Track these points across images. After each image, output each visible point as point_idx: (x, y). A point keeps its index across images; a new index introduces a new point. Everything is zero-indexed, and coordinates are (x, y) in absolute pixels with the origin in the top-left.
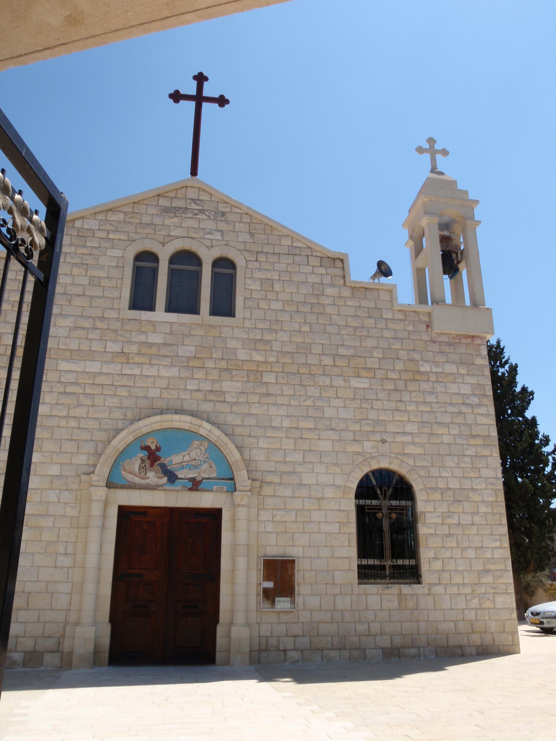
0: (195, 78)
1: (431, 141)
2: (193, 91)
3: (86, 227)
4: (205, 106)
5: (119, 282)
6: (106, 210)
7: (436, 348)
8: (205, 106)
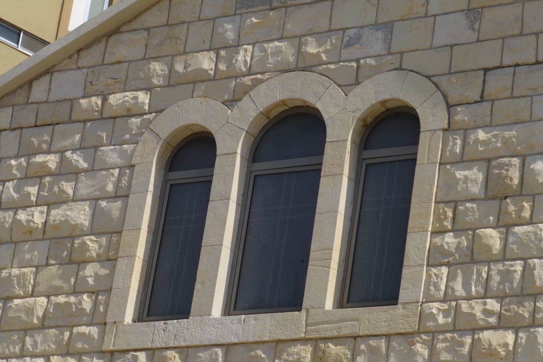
3: (57, 94)
6: (103, 36)
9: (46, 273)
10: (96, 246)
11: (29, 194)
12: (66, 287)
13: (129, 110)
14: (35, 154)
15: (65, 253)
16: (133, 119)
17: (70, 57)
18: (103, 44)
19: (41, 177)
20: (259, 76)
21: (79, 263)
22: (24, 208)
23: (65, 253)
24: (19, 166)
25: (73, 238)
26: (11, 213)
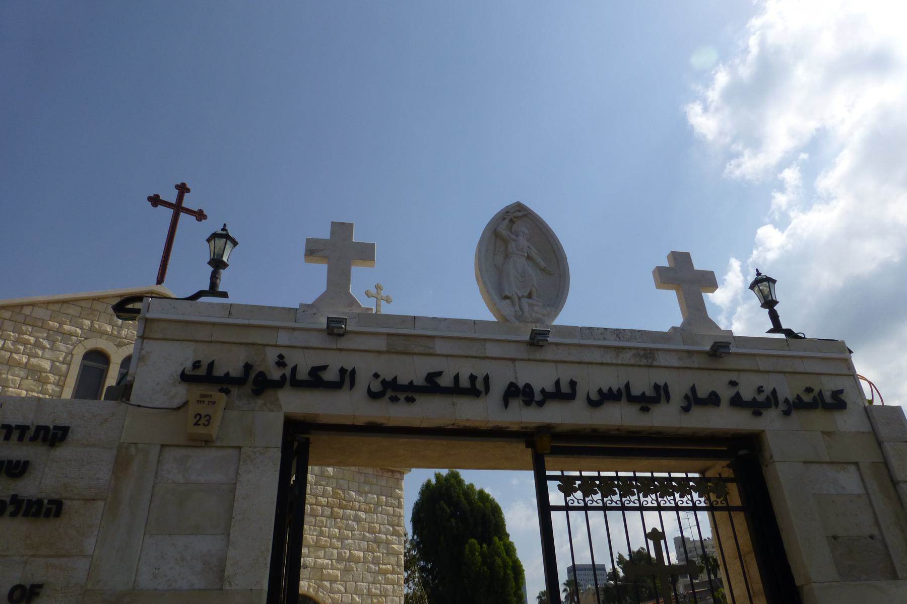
0: (177, 187)
1: (378, 287)
2: (173, 200)
4: (183, 216)
5: (63, 378)
7: (362, 479)
8: (183, 216)
9: (25, 382)
10: (53, 379)
11: (20, 349)
12: (36, 389)
13: (71, 333)
14: (23, 334)
15: (36, 377)
16: (73, 337)
17: (44, 303)
18: (60, 305)
19: (25, 344)
20: (130, 341)
21: (43, 383)
22: (16, 353)
23: (36, 377)
24: (15, 336)
25: (41, 372)
26: (9, 353)
